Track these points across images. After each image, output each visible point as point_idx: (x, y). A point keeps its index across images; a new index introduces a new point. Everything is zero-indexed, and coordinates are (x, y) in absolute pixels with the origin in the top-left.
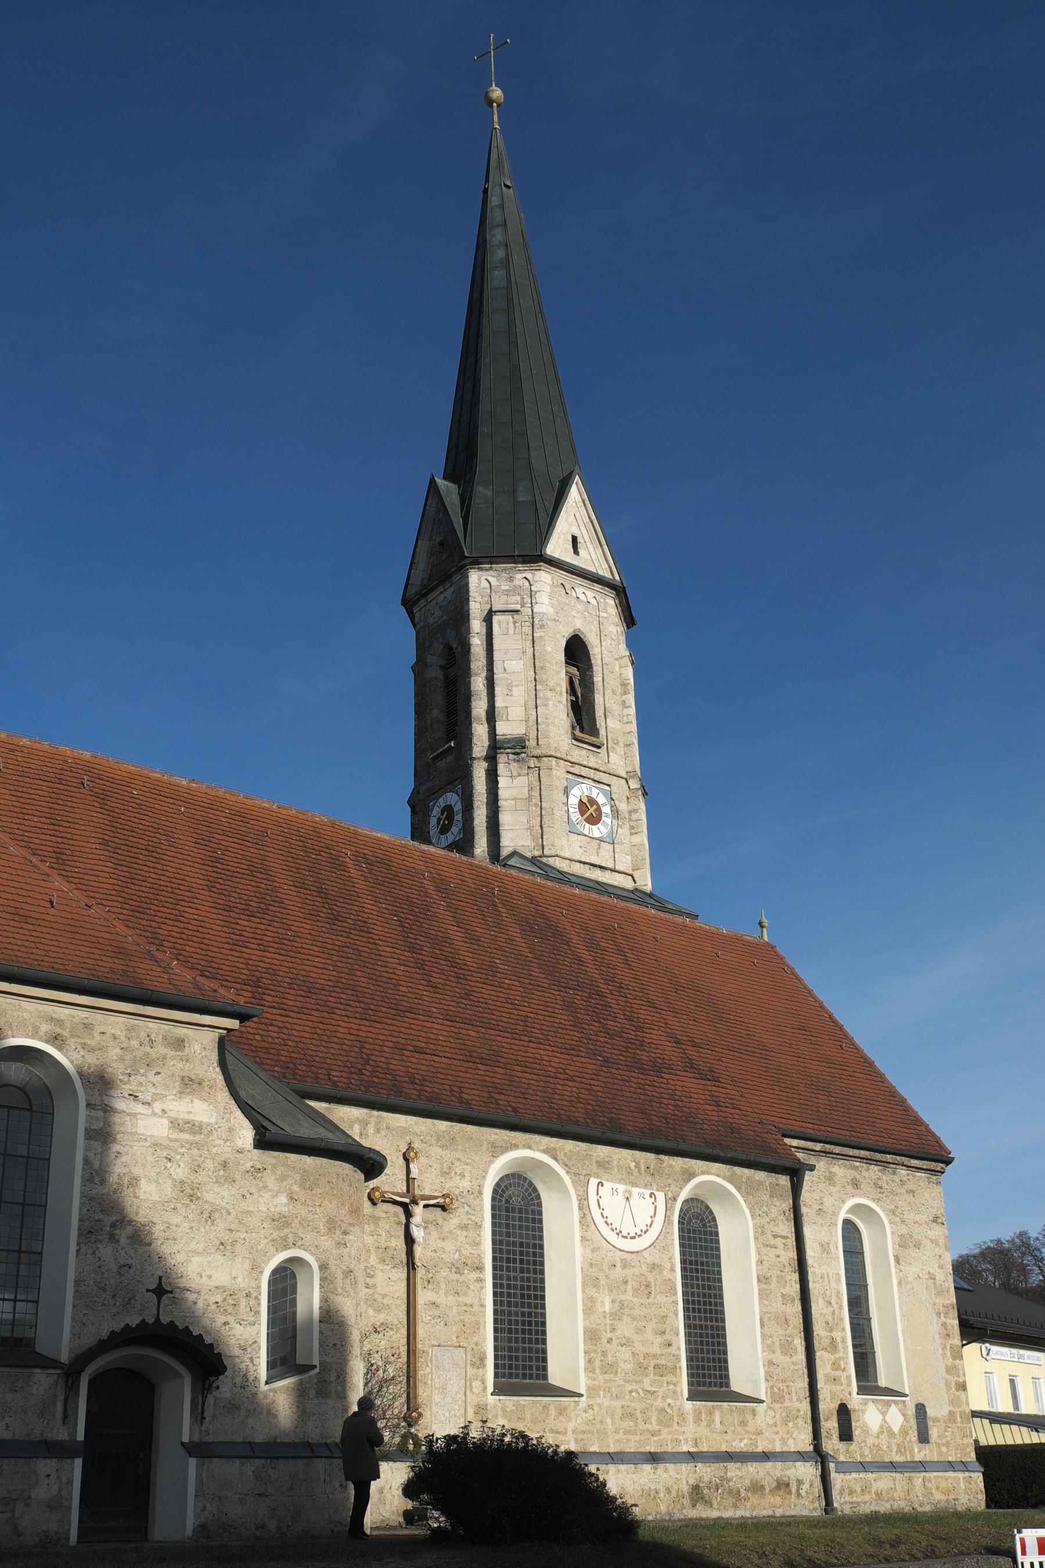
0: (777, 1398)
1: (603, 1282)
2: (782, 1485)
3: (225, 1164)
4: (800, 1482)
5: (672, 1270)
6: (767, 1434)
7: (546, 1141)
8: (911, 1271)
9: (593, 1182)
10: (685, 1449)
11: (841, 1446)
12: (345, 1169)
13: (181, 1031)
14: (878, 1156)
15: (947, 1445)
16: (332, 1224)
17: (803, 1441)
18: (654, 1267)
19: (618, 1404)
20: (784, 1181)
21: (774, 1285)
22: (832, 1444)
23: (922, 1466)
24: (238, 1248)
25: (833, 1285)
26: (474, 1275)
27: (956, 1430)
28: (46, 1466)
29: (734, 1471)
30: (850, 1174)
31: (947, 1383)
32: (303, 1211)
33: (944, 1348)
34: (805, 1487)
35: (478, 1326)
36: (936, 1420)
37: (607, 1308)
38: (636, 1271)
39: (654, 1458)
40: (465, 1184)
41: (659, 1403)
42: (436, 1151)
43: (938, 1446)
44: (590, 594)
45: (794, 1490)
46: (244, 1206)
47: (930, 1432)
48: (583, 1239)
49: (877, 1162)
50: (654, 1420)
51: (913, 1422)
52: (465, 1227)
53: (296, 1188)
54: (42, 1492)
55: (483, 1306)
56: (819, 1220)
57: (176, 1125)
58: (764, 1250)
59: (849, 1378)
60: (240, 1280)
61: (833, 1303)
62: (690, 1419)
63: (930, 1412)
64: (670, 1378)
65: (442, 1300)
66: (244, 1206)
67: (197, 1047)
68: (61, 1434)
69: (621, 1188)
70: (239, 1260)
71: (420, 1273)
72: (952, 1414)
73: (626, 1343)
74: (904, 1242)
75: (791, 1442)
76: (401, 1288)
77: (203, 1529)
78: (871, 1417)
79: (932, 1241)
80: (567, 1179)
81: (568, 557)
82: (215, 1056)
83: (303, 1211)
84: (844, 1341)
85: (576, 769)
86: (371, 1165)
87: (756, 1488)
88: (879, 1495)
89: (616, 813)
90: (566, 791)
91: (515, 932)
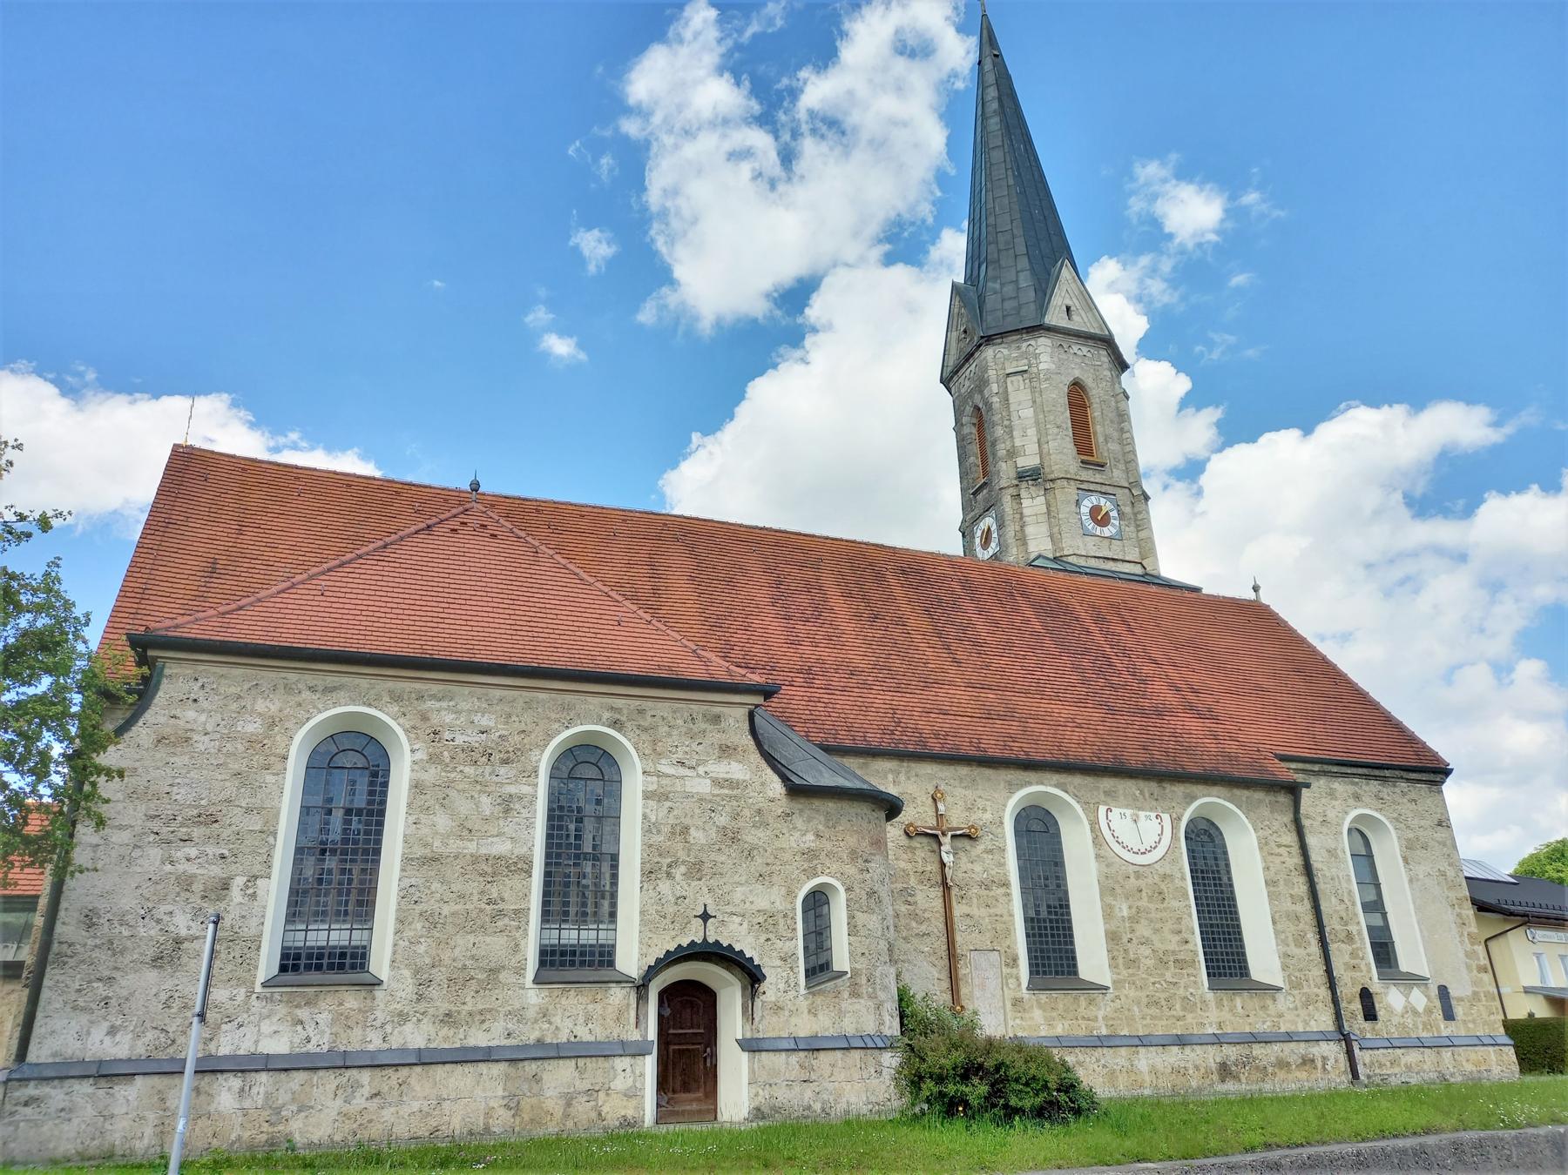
0: (1296, 985)
1: (1119, 891)
2: (1308, 1062)
3: (759, 811)
4: (1324, 1059)
5: (1183, 879)
6: (1289, 1016)
7: (1056, 778)
8: (1421, 870)
9: (1102, 809)
10: (1210, 1031)
11: (1368, 1025)
12: (863, 809)
13: (717, 710)
14: (1377, 772)
15: (1474, 1021)
16: (854, 855)
17: (1324, 1020)
18: (1164, 877)
19: (1143, 994)
20: (1284, 799)
21: (1281, 887)
22: (1356, 1024)
23: (1450, 1043)
24: (775, 878)
25: (1344, 885)
26: (1002, 890)
28: (621, 1063)
29: (1257, 1050)
30: (1351, 789)
31: (1468, 967)
32: (828, 846)
33: (1462, 935)
34: (1331, 1062)
35: (1008, 932)
36: (1461, 999)
37: (1125, 913)
38: (1150, 881)
39: (1181, 1041)
40: (988, 816)
41: (1181, 992)
42: (959, 792)
44: (1085, 350)
45: (1319, 1064)
46: (777, 844)
48: (1098, 856)
49: (1376, 778)
50: (1178, 1006)
51: (1438, 1003)
52: (990, 852)
53: (821, 827)
54: (620, 1084)
55: (1012, 915)
56: (1324, 830)
57: (717, 782)
58: (1270, 858)
59: (1368, 965)
60: (778, 904)
62: (1213, 1004)
63: (1453, 992)
64: (1191, 971)
65: (975, 911)
66: (777, 844)
67: (731, 720)
68: (635, 1036)
69: (1128, 812)
70: (775, 888)
71: (955, 891)
72: (1475, 993)
73: (1145, 942)
74: (1409, 846)
75: (1313, 1023)
76: (938, 904)
77: (758, 1113)
78: (1392, 999)
80: (1077, 807)
81: (1063, 322)
82: (746, 726)
83: (828, 846)
84: (1360, 933)
86: (892, 808)
87: (1283, 1064)
88: (1409, 1068)
89: (1121, 515)
90: (1078, 503)
91: (1029, 613)
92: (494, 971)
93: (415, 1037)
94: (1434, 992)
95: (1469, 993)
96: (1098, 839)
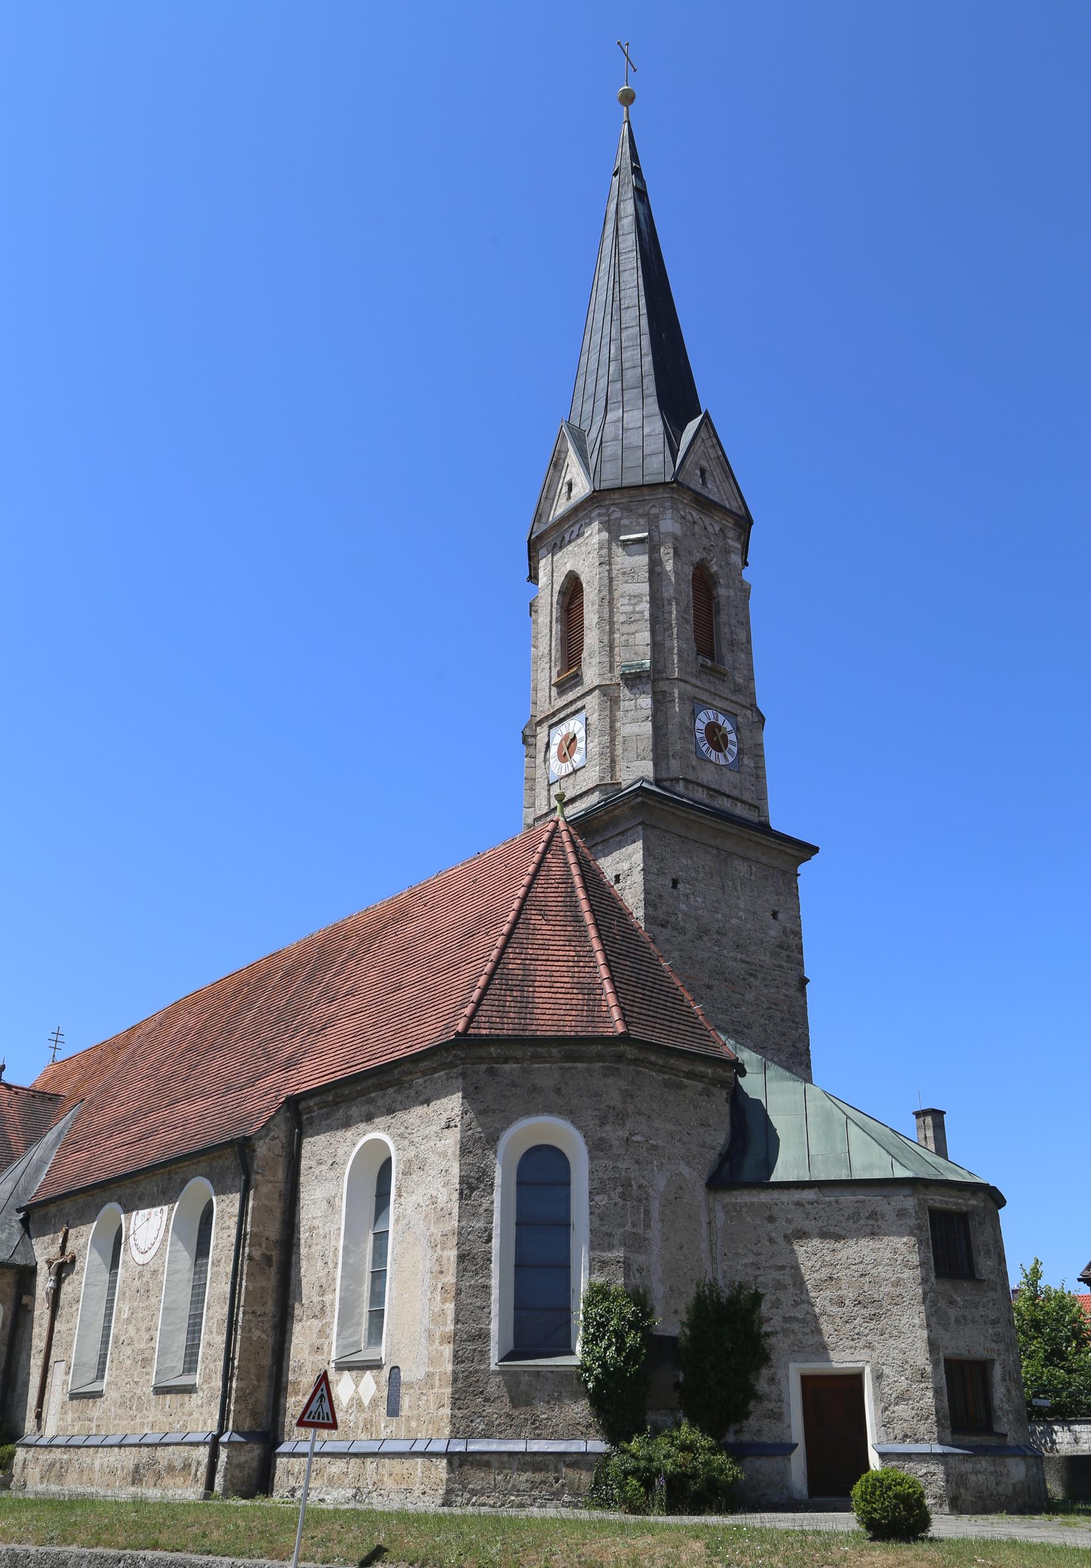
6: (196, 1415)
25: (333, 1242)
27: (431, 1399)
31: (430, 1336)
36: (410, 1385)
43: (408, 1419)
47: (401, 1402)
61: (331, 1265)
63: (404, 1376)
72: (429, 1375)
79: (439, 1154)
84: (332, 1305)
87: (171, 1468)
94: (386, 1371)
95: (421, 1375)
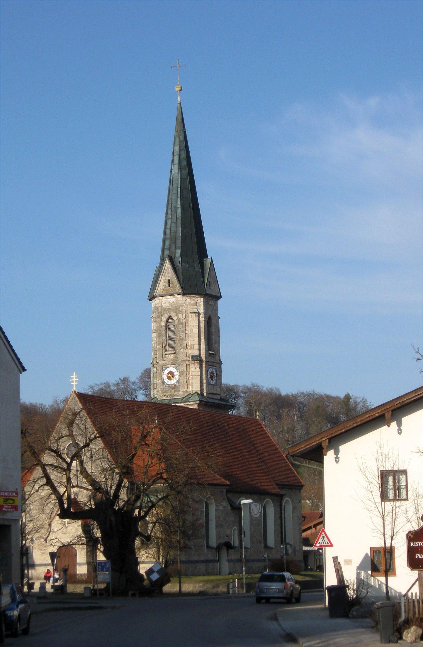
28: (216, 564)
85: (209, 364)
92: (202, 546)
93: (196, 558)
94: (293, 548)
96: (250, 512)
